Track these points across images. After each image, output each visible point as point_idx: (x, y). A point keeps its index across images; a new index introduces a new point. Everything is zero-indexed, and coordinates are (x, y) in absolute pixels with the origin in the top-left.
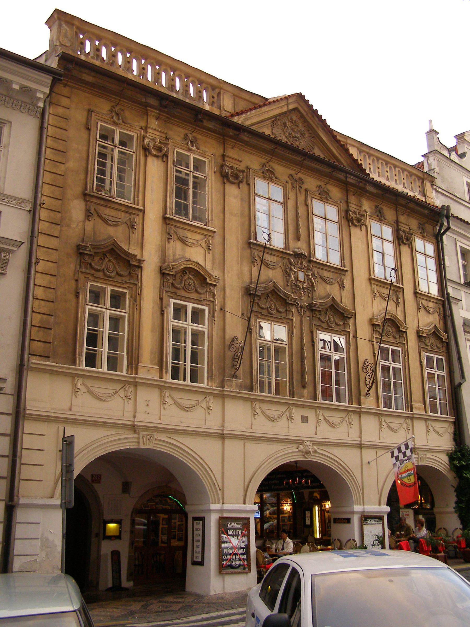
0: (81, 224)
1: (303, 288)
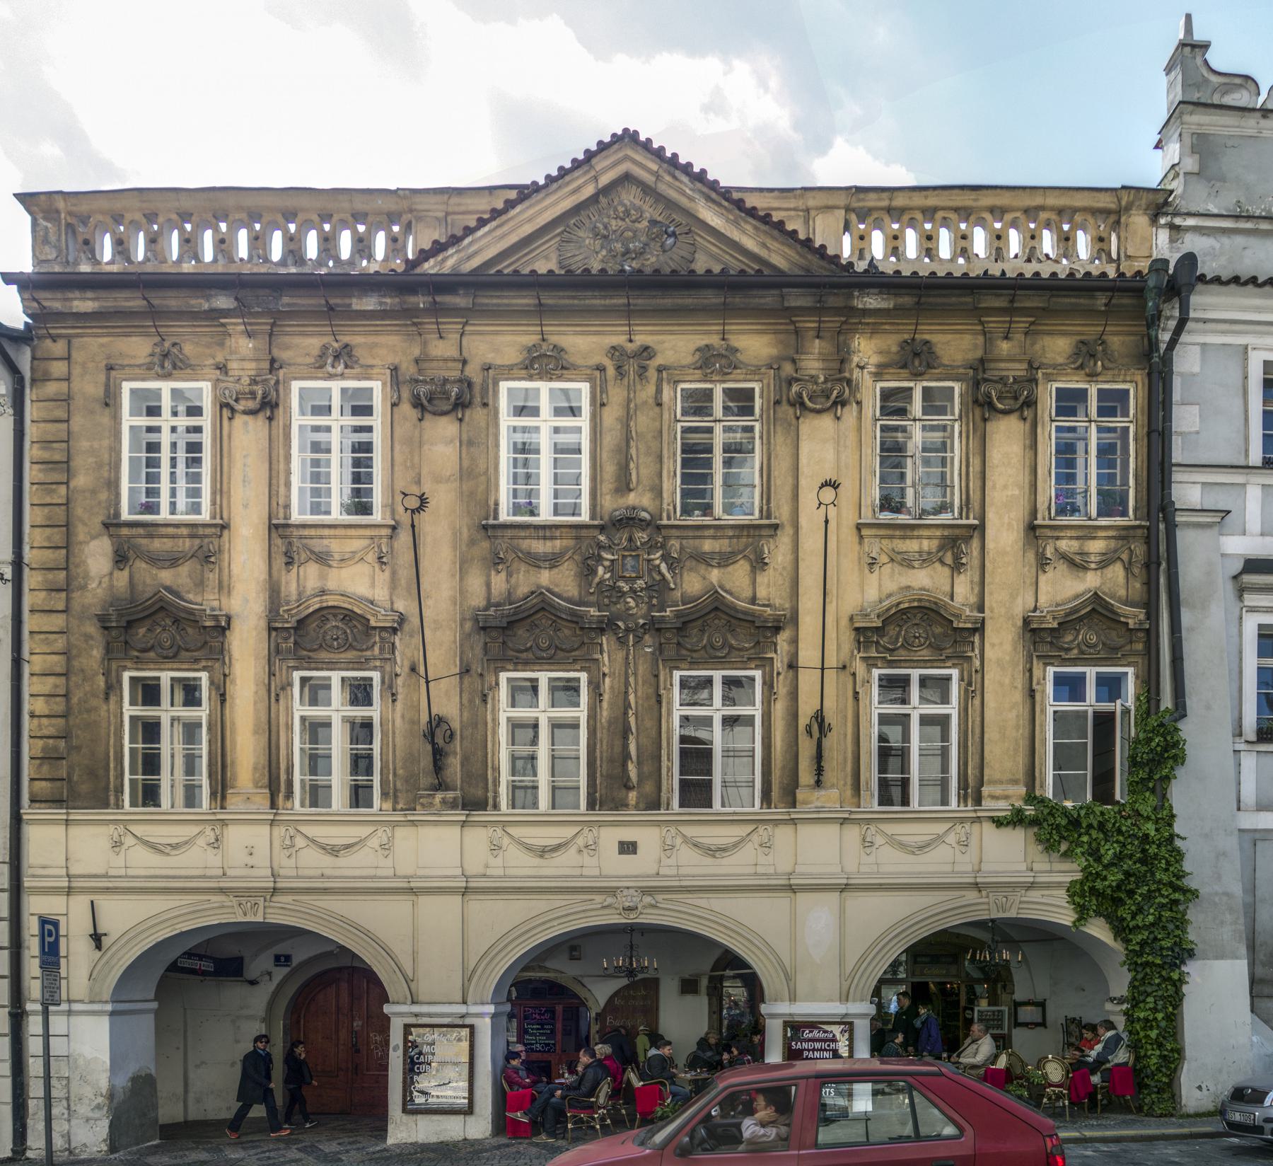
0: (106, 579)
1: (633, 591)
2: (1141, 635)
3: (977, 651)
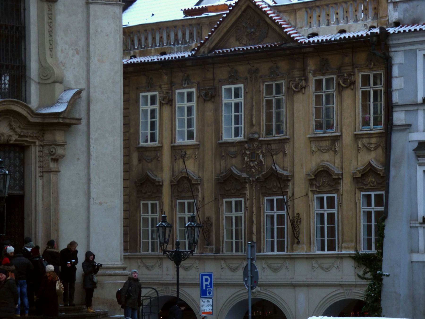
3: (341, 187)
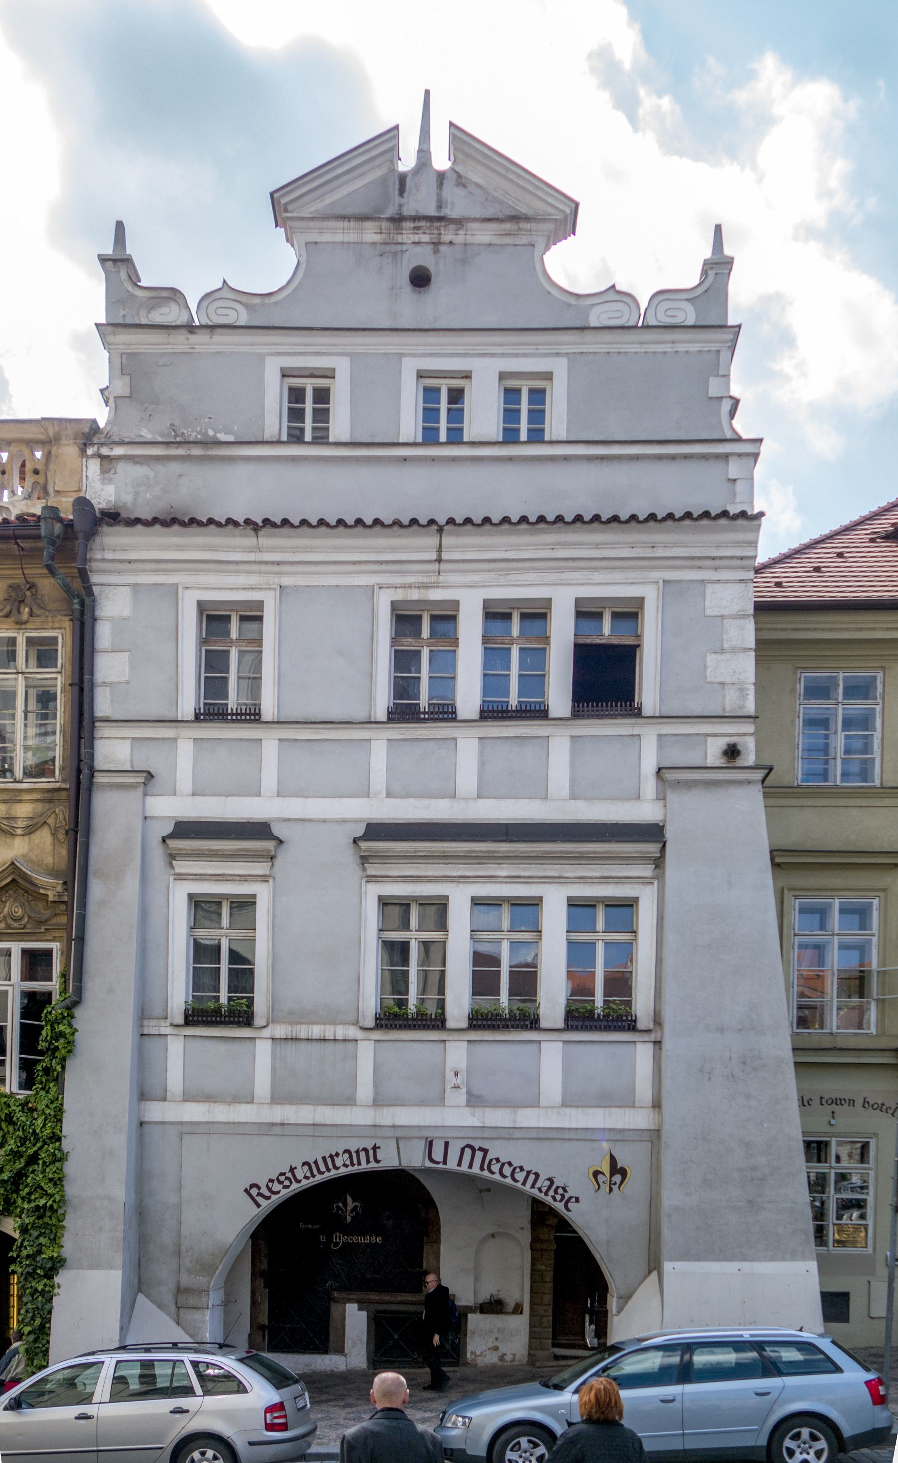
2: (63, 907)
